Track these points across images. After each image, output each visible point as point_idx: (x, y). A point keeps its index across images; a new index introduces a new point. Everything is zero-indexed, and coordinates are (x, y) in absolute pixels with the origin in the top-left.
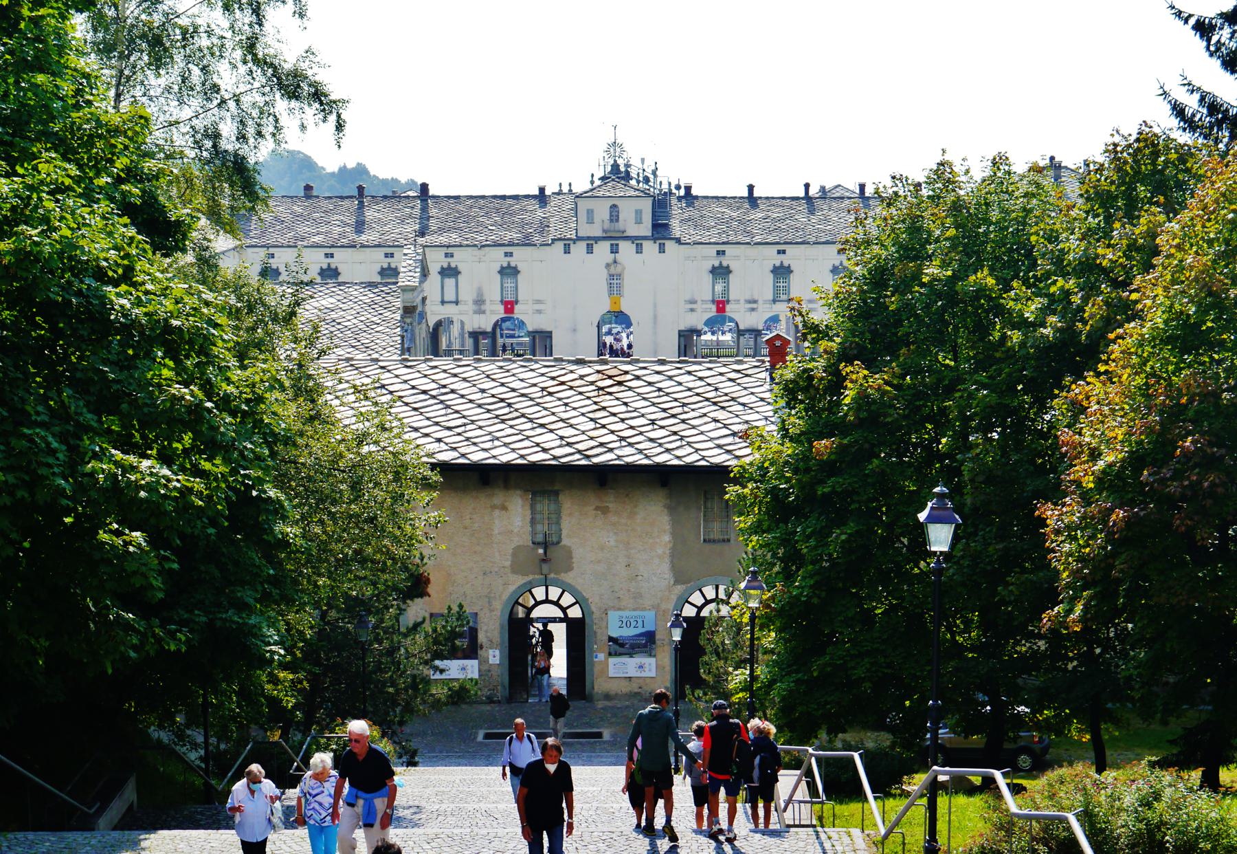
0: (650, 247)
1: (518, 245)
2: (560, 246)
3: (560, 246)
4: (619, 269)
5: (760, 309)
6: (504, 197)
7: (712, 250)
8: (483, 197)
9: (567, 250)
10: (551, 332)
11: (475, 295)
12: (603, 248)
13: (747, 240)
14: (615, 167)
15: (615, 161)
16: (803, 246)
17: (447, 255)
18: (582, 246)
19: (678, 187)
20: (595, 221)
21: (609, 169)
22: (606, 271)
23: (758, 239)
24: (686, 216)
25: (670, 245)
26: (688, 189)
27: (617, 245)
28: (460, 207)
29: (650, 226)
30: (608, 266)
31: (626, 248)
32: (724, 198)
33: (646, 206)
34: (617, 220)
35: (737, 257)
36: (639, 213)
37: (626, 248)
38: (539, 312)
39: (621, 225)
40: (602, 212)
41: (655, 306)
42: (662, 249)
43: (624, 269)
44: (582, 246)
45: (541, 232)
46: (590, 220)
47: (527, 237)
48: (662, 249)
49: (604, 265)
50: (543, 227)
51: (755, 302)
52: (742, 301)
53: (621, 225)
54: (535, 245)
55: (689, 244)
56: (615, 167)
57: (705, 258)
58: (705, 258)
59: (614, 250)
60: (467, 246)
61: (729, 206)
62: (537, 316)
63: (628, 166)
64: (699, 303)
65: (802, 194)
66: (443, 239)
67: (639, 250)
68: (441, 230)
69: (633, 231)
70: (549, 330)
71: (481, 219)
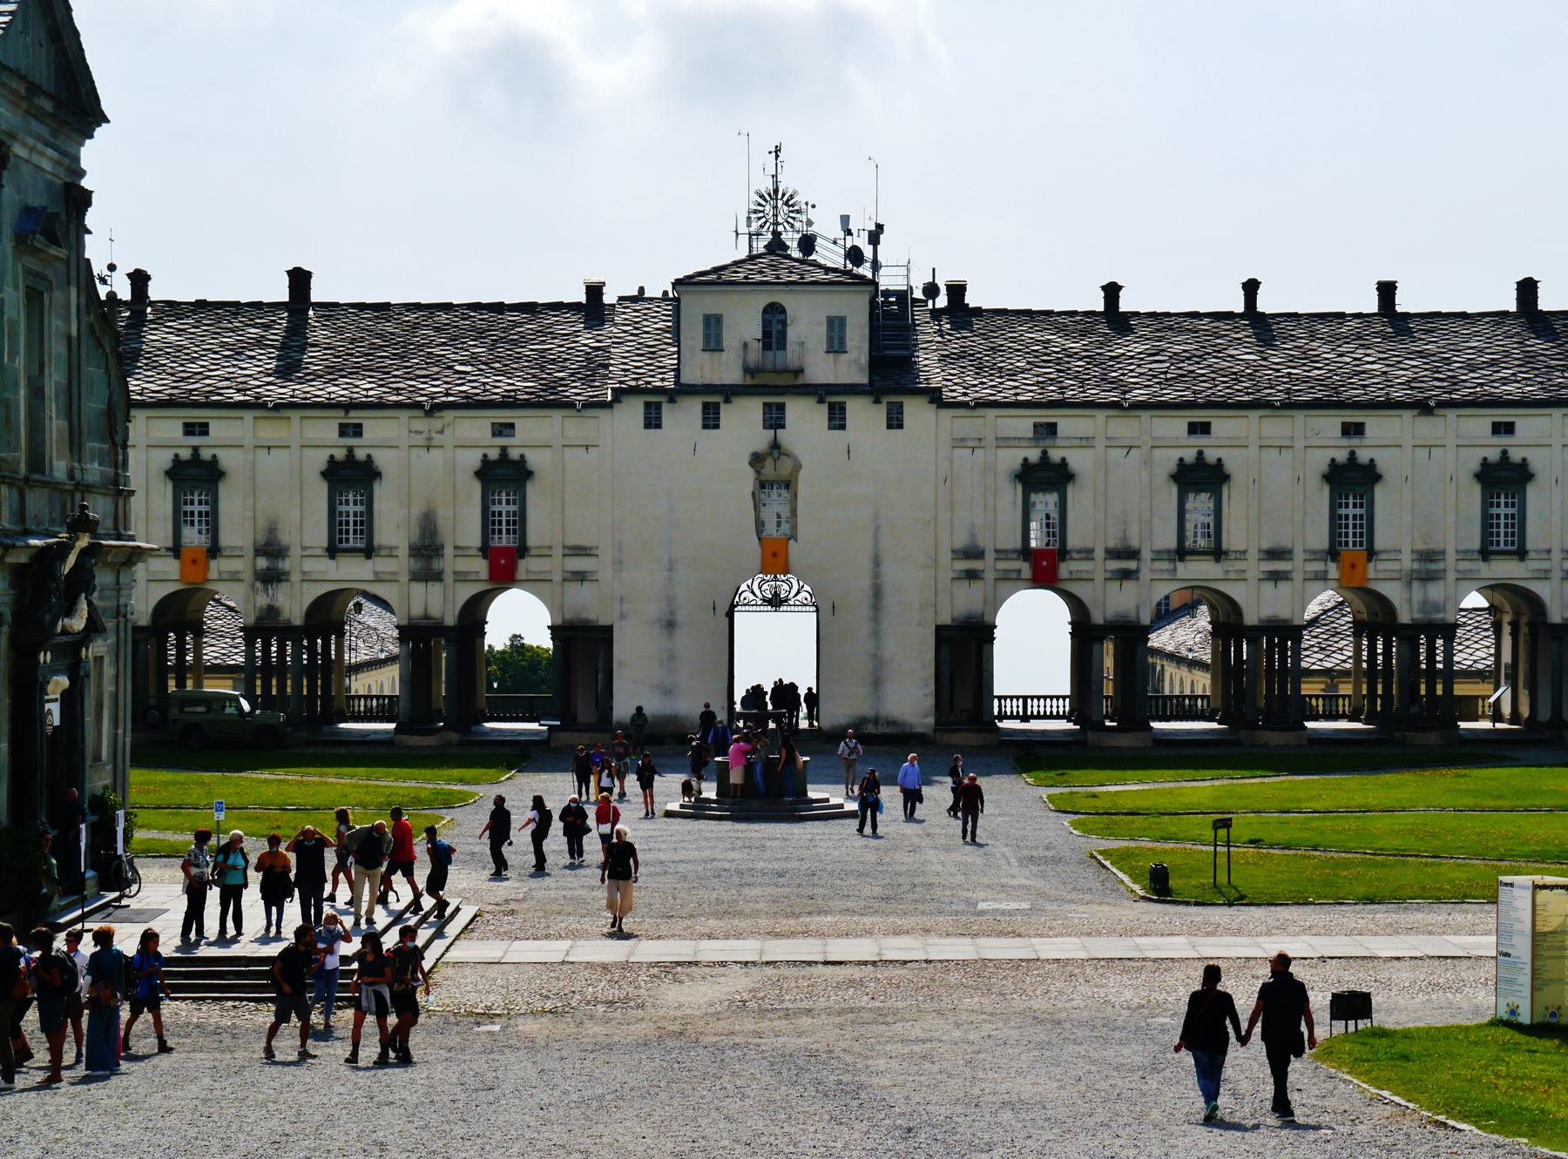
0: (864, 415)
1: (527, 405)
2: (634, 409)
3: (634, 409)
4: (785, 467)
5: (1145, 574)
6: (499, 308)
7: (1022, 424)
8: (447, 307)
9: (653, 421)
10: (609, 630)
11: (415, 533)
12: (742, 422)
13: (1113, 397)
14: (777, 245)
15: (776, 234)
16: (1254, 415)
17: (344, 430)
18: (692, 409)
19: (931, 290)
20: (725, 344)
21: (760, 246)
22: (750, 473)
23: (1139, 395)
24: (954, 347)
25: (916, 411)
26: (957, 291)
27: (781, 408)
28: (389, 327)
29: (864, 359)
30: (757, 460)
31: (804, 417)
32: (1049, 313)
33: (856, 311)
34: (782, 345)
35: (1086, 442)
36: (836, 326)
37: (804, 417)
38: (580, 577)
39: (791, 356)
40: (745, 322)
41: (877, 562)
42: (895, 421)
43: (797, 467)
44: (692, 409)
45: (587, 380)
46: (713, 343)
47: (551, 387)
48: (895, 421)
49: (747, 458)
50: (594, 366)
51: (1133, 554)
52: (1099, 554)
53: (791, 356)
54: (571, 405)
55: (964, 405)
56: (777, 245)
57: (1004, 442)
58: (1004, 442)
59: (775, 419)
60: (398, 405)
61: (1061, 329)
62: (573, 589)
63: (808, 243)
64: (990, 556)
65: (1239, 308)
66: (337, 391)
67: (837, 419)
68: (332, 373)
69: (822, 369)
70: (603, 621)
71: (436, 351)
